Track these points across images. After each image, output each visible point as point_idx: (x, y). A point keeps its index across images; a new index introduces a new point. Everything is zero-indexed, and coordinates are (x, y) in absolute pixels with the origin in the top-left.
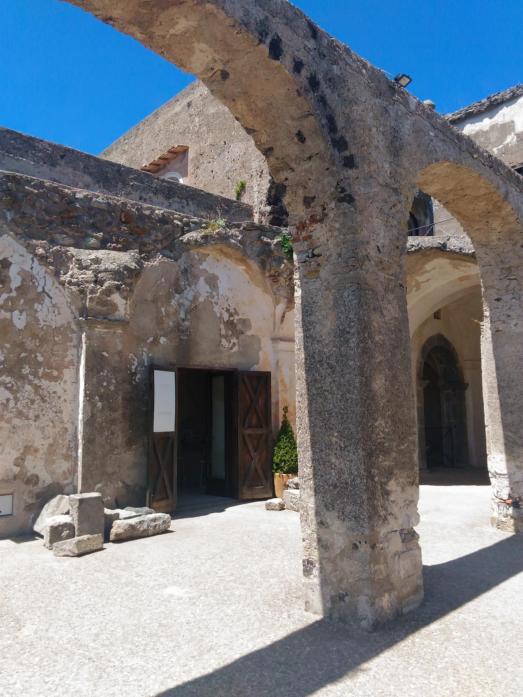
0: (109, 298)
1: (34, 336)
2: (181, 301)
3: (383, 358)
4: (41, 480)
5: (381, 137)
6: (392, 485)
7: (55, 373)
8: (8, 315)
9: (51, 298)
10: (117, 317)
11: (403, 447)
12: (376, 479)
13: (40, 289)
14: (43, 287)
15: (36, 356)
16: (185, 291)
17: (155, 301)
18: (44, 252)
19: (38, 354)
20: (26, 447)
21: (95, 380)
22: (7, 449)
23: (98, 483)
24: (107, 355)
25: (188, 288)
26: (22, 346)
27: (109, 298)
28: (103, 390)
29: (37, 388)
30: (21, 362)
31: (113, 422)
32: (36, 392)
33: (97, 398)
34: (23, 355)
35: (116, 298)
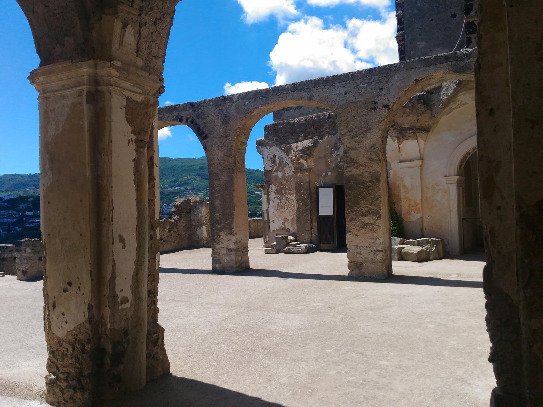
0: (299, 162)
1: (285, 180)
2: (338, 153)
3: (219, 194)
4: (291, 231)
5: (219, 121)
6: (221, 233)
7: (292, 192)
8: (276, 173)
9: (289, 165)
10: (305, 168)
11: (226, 222)
12: (215, 231)
13: (285, 162)
14: (286, 161)
15: (286, 187)
16: (340, 148)
17: (325, 157)
18: (284, 148)
19: (286, 186)
20: (285, 219)
21: (299, 194)
22: (280, 219)
23: (303, 234)
24: (303, 184)
25: (342, 146)
26: (281, 183)
27: (299, 162)
28: (302, 198)
29: (287, 198)
30: (281, 189)
31: (307, 210)
32: (286, 200)
33: (300, 201)
34: (282, 187)
35: (302, 161)
